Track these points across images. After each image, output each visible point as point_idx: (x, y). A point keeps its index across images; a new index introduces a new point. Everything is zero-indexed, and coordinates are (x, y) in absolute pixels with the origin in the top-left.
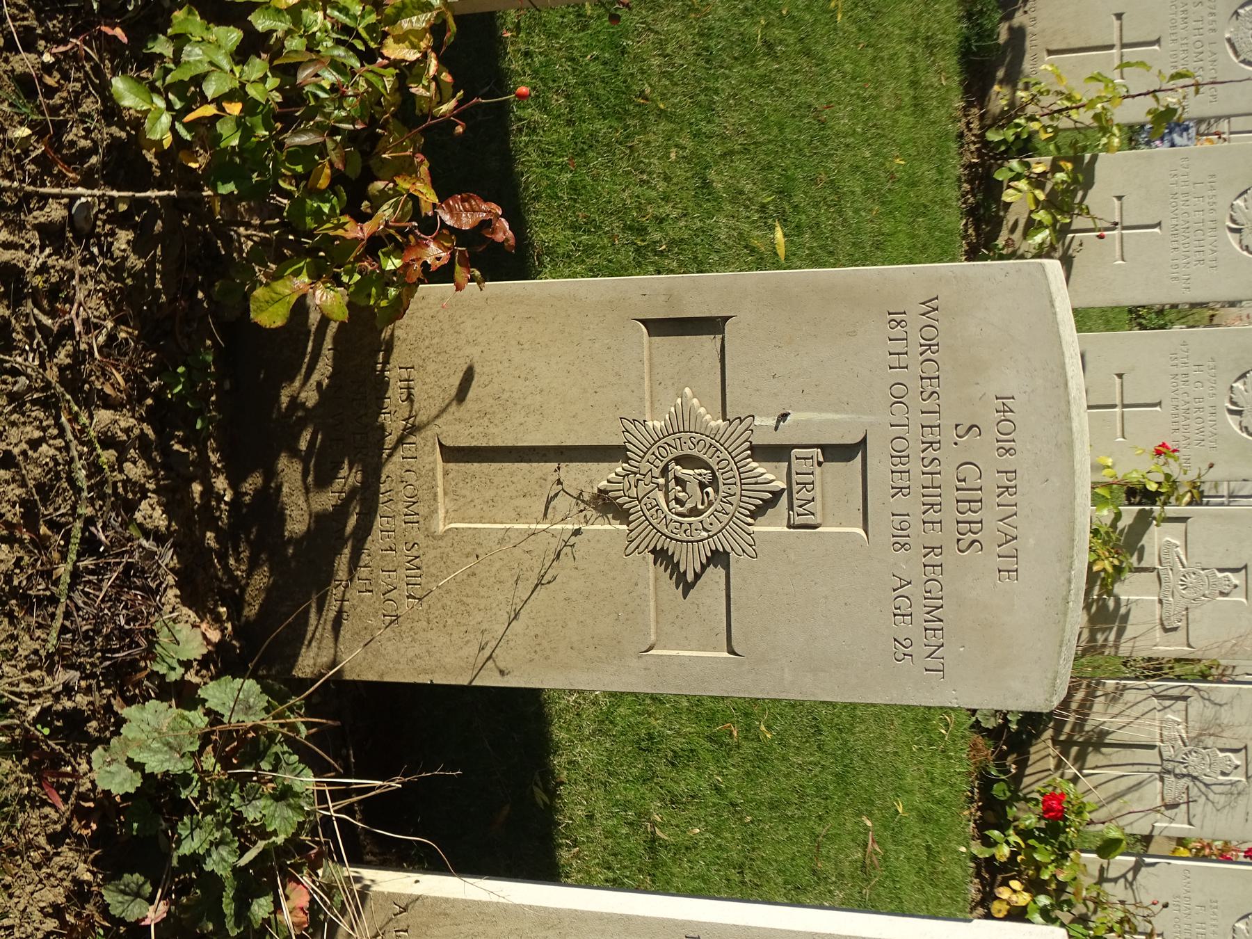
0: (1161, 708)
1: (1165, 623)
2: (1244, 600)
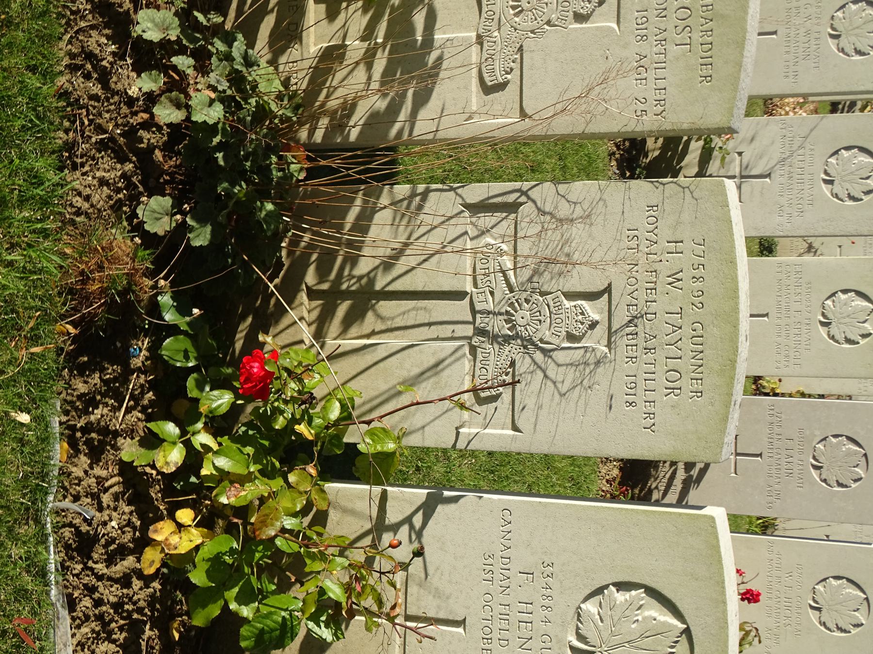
0: (476, 233)
1: (487, 79)
2: (614, 25)
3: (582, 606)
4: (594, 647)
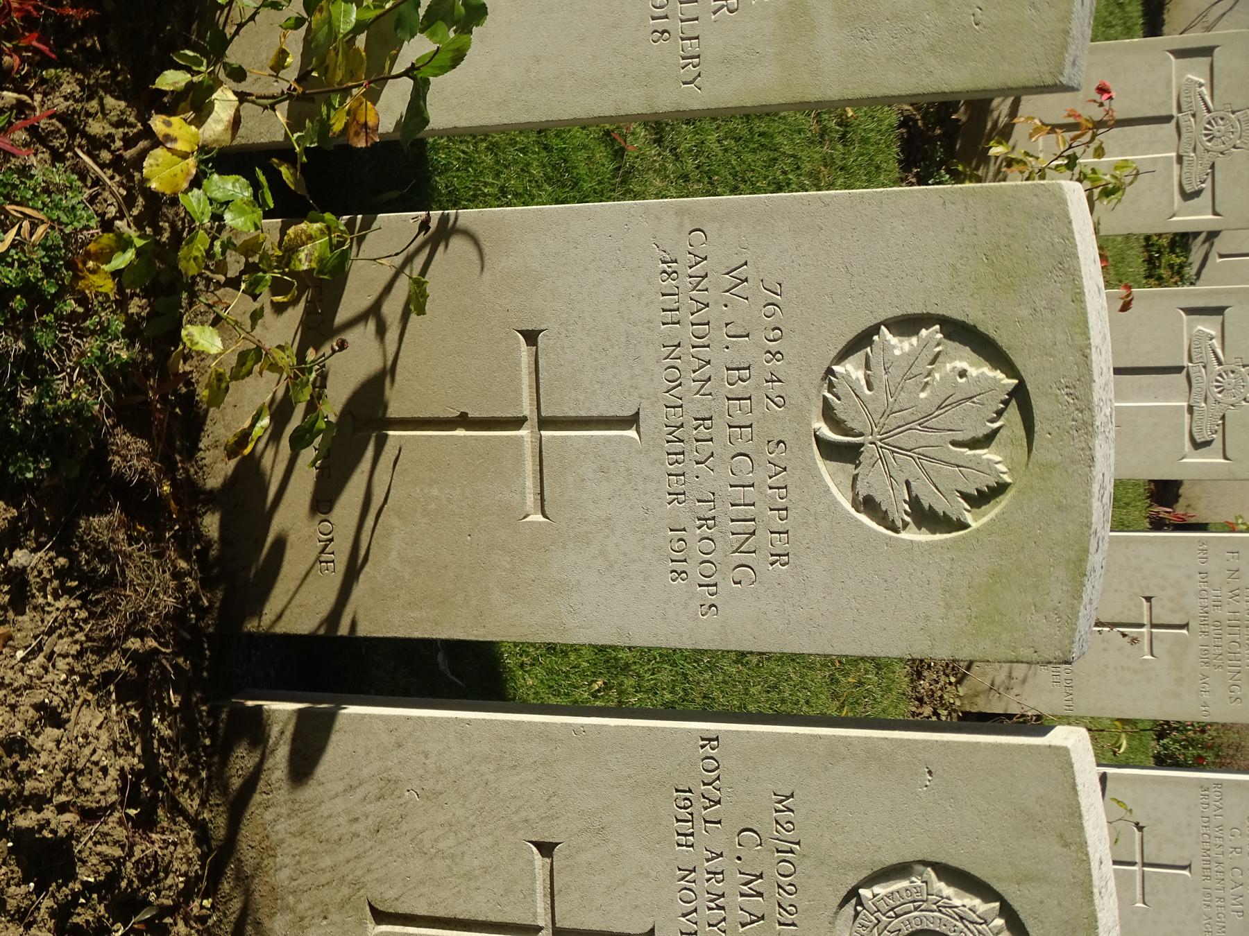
3: (835, 368)
4: (861, 435)
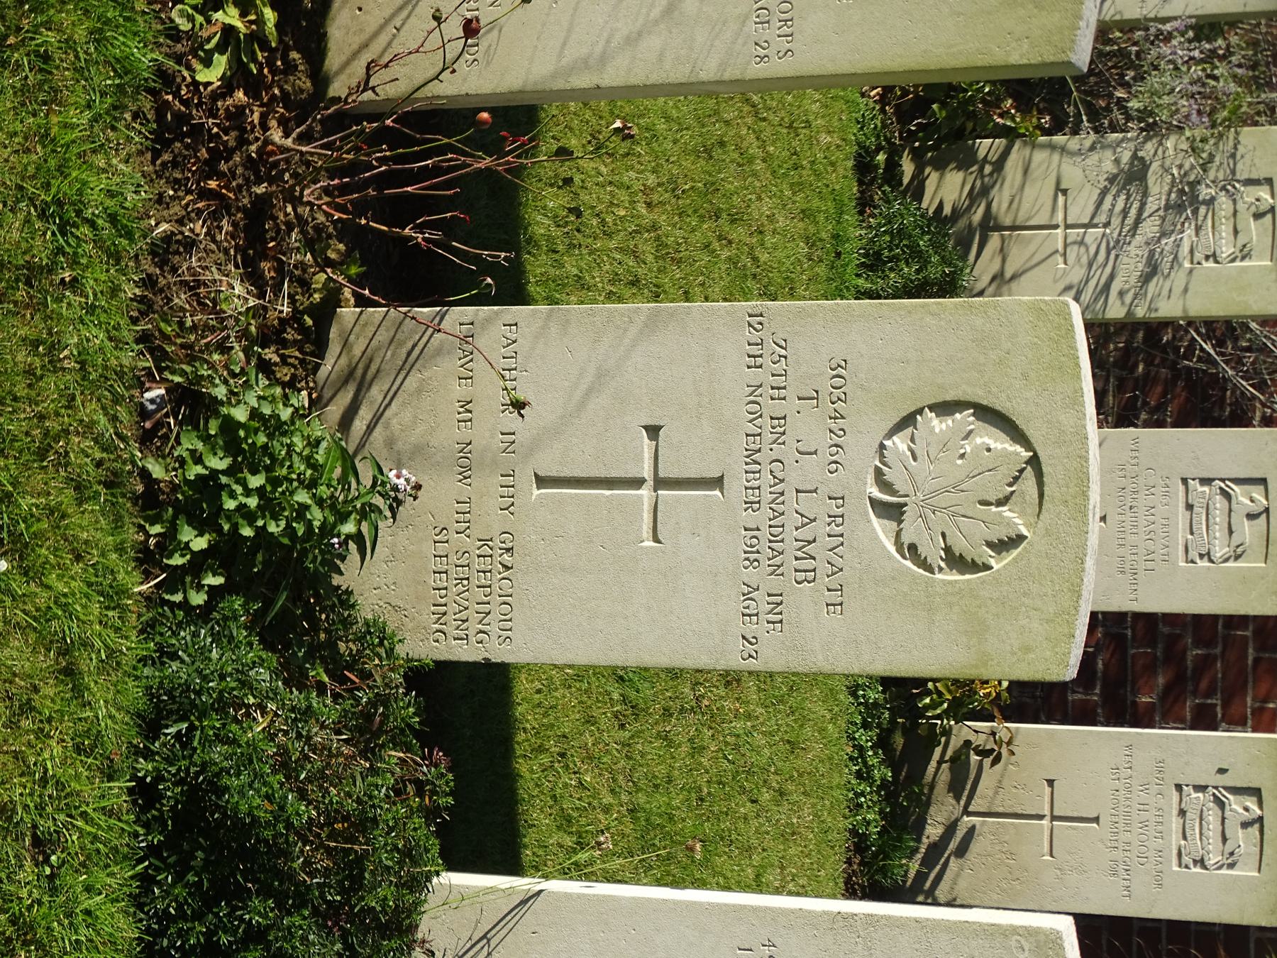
3: (885, 442)
4: (907, 496)
